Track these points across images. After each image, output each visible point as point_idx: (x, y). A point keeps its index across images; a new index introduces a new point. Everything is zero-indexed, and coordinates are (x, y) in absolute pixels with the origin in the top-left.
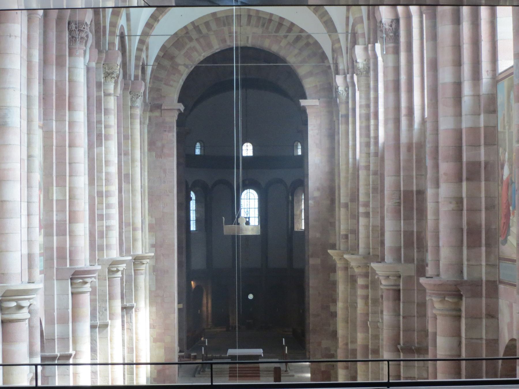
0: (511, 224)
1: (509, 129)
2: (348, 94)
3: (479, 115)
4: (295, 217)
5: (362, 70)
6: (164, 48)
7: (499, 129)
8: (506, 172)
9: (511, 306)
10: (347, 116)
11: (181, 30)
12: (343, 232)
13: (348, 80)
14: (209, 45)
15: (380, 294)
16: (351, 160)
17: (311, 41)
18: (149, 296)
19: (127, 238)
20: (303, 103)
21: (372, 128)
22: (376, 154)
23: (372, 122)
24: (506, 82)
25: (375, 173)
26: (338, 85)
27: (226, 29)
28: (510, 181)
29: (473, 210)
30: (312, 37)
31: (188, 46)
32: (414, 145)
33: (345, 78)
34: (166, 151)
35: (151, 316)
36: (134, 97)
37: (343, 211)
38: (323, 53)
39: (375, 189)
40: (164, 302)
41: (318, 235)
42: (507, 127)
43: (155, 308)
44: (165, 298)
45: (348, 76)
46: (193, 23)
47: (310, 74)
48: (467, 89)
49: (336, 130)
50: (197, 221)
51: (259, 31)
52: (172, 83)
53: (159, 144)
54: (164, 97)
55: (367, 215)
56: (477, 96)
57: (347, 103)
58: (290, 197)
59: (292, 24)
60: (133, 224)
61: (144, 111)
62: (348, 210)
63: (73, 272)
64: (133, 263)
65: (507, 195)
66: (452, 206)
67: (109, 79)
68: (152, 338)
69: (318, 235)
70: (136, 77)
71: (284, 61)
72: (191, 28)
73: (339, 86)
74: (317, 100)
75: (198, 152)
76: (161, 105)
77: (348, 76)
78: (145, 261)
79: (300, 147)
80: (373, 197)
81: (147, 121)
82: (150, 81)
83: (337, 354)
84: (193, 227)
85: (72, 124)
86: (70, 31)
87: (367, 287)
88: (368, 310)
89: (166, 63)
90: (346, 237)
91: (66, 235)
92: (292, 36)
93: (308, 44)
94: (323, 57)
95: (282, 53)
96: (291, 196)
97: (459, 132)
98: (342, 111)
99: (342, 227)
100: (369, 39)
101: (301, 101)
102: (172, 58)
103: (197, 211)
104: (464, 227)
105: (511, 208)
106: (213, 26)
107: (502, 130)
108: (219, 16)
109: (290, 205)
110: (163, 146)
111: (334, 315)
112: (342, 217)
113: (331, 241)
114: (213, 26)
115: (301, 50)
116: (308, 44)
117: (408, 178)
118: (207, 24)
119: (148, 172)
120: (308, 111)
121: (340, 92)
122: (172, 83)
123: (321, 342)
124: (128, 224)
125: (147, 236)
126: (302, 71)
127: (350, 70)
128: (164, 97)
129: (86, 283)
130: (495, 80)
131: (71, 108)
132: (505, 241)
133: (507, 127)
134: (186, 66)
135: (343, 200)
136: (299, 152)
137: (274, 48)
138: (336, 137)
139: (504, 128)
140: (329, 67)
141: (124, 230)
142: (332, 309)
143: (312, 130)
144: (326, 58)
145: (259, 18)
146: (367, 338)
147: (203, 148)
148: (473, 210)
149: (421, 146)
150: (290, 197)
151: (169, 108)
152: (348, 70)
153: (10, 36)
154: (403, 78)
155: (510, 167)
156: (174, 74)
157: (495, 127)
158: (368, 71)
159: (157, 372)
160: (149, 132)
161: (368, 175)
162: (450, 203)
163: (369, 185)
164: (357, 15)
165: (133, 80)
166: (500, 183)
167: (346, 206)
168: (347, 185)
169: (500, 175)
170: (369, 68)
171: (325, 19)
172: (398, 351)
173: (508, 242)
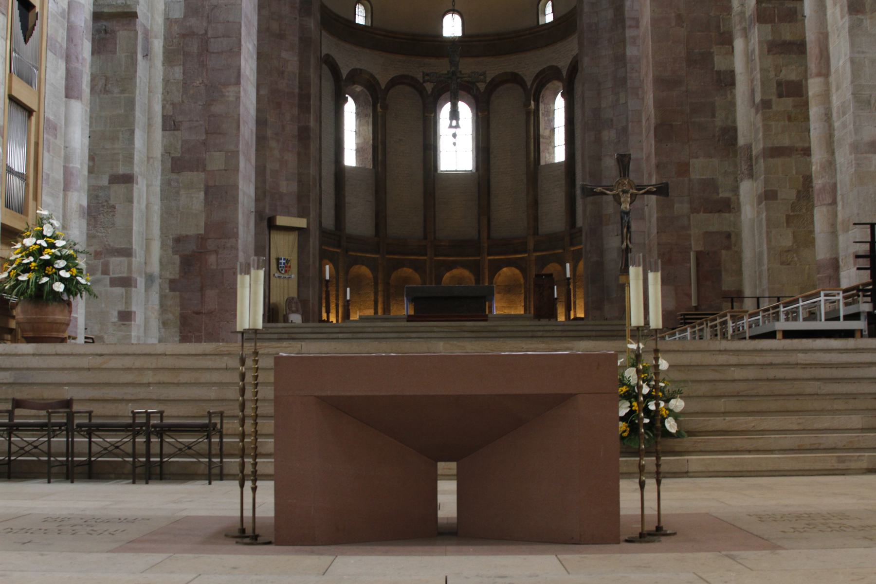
4: (541, 140)
18: (164, 35)
35: (168, 93)
40: (207, 51)
43: (182, 71)
44: (212, 40)
50: (359, 151)
58: (532, 103)
68: (170, 160)
75: (360, 19)
79: (549, 9)
83: (738, 199)
84: (350, 159)
96: (534, 101)
103: (358, 133)
109: (532, 118)
111: (727, 80)
123: (687, 164)
136: (549, 18)
142: (720, 63)
147: (371, 13)
150: (532, 103)
159: (181, 262)
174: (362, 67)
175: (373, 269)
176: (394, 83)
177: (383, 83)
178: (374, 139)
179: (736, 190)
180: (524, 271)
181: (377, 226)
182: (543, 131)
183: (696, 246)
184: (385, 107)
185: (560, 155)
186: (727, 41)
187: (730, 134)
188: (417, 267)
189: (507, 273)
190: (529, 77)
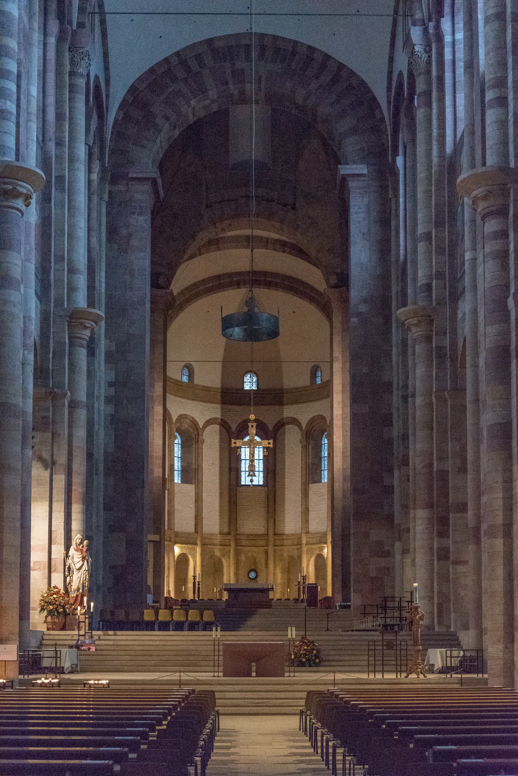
2: (430, 57)
6: (133, 90)
10: (428, 94)
11: (159, 64)
12: (421, 281)
16: (435, 160)
19: (59, 281)
20: (345, 170)
26: (415, 42)
27: (227, 64)
30: (358, 77)
31: (170, 89)
34: (134, 242)
36: (76, 55)
38: (374, 99)
46: (177, 54)
47: (354, 131)
49: (393, 212)
53: (124, 232)
54: (133, 162)
57: (429, 72)
59: (328, 57)
60: (70, 262)
61: (102, 179)
62: (431, 243)
64: (66, 323)
70: (81, 25)
72: (175, 61)
73: (415, 45)
74: (365, 166)
76: (128, 173)
78: (89, 323)
81: (106, 197)
82: (111, 137)
92: (326, 78)
98: (420, 86)
99: (420, 273)
101: (340, 166)
106: (209, 61)
110: (130, 235)
114: (209, 61)
118: (199, 57)
119: (106, 272)
120: (352, 184)
121: (417, 54)
122: (145, 142)
124: (60, 259)
125: (103, 368)
128: (133, 162)
134: (167, 118)
138: (393, 223)
140: (382, 119)
141: (52, 264)
143: (356, 213)
144: (378, 106)
151: (140, 175)
156: (149, 130)
160: (108, 213)
163: (506, 47)
165: (75, 28)
167: (428, 237)
174: (188, 413)
181: (196, 525)
186: (391, 471)
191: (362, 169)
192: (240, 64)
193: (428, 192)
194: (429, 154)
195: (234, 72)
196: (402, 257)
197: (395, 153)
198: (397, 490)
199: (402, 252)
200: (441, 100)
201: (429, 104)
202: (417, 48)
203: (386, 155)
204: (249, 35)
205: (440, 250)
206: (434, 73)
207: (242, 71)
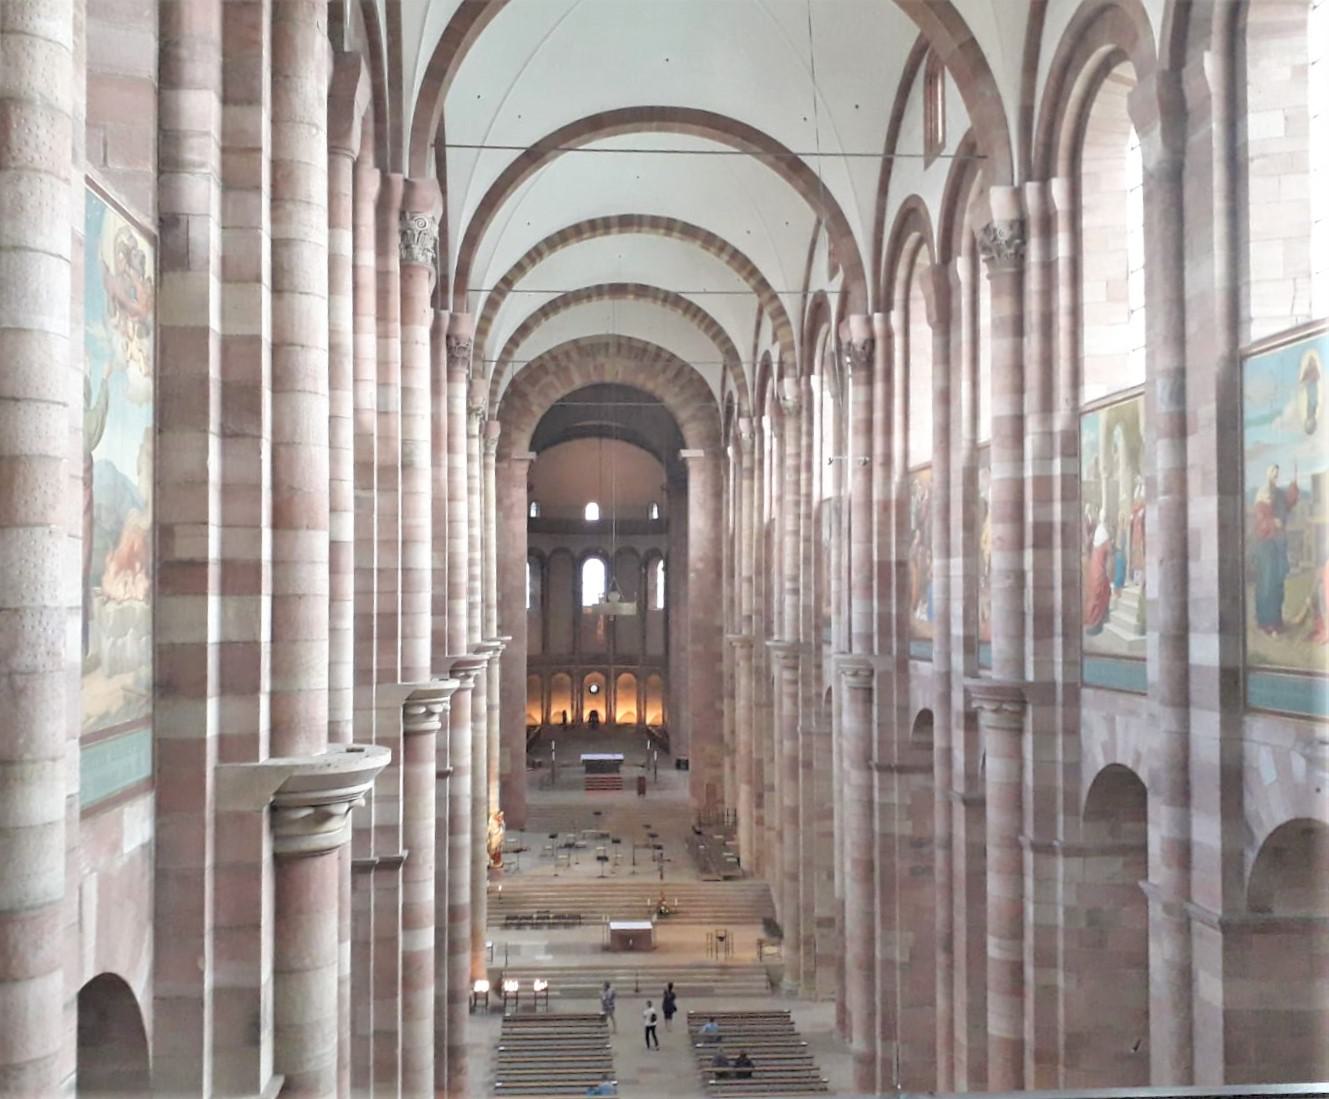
0: (1111, 607)
1: (1110, 475)
3: (1051, 458)
5: (791, 410)
7: (1085, 477)
8: (1100, 536)
9: (1111, 721)
10: (752, 471)
12: (745, 612)
13: (755, 423)
14: (573, 383)
15: (814, 691)
17: (695, 377)
20: (684, 453)
21: (803, 483)
22: (808, 516)
23: (803, 476)
24: (1103, 415)
25: (807, 540)
28: (1109, 548)
29: (1043, 586)
32: (893, 504)
33: (751, 422)
34: (516, 511)
37: (745, 586)
39: (807, 559)
41: (701, 615)
42: (1104, 476)
45: (755, 420)
46: (549, 352)
47: (694, 417)
48: (1032, 425)
49: (725, 487)
51: (632, 364)
52: (523, 426)
55: (796, 591)
56: (1048, 434)
57: (753, 453)
63: (453, 662)
65: (1104, 566)
66: (1009, 582)
67: (474, 414)
69: (701, 615)
71: (660, 400)
72: (547, 357)
77: (755, 420)
79: (655, 509)
80: (804, 569)
85: (451, 471)
86: (449, 349)
87: (795, 682)
88: (797, 711)
89: (517, 403)
90: (750, 618)
91: (444, 613)
92: (670, 373)
93: (691, 380)
94: (710, 396)
95: (658, 393)
97: (1019, 485)
99: (745, 606)
100: (802, 370)
102: (523, 396)
104: (1026, 609)
105: (1112, 586)
107: (1092, 479)
108: (582, 343)
111: (721, 713)
112: (745, 595)
113: (717, 623)
114: (574, 355)
115: (682, 388)
116: (691, 380)
117: (884, 547)
118: (567, 354)
120: (690, 464)
126: (683, 415)
127: (757, 413)
129: (468, 677)
130: (1077, 414)
131: (451, 449)
132: (1098, 629)
133: (1104, 476)
134: (540, 405)
135: (745, 573)
136: (655, 515)
137: (650, 386)
139: (1097, 476)
140: (717, 410)
142: (718, 705)
145: (631, 348)
146: (796, 749)
148: (1043, 586)
149: (903, 505)
152: (754, 411)
153: (417, 343)
154: (878, 415)
155: (1111, 529)
157: (1078, 476)
158: (799, 413)
161: (798, 543)
162: (1008, 577)
164: (787, 340)
166: (1084, 550)
167: (750, 580)
168: (751, 557)
169: (1086, 539)
170: (801, 407)
171: (727, 346)
172: (869, 768)
173: (1105, 631)
175: (541, 676)
176: (555, 552)
177: (547, 553)
178: (542, 590)
179: (722, 759)
180: (636, 676)
181: (543, 647)
182: (650, 587)
183: (706, 781)
184: (548, 570)
185: (660, 604)
187: (721, 738)
188: (569, 673)
189: (625, 677)
190: (642, 553)
191: (700, 453)
192: (601, 359)
193: (751, 546)
194: (751, 517)
195: (595, 368)
196: (731, 531)
197: (727, 445)
198: (726, 713)
199: (731, 525)
200: (761, 477)
201: (752, 478)
202: (744, 435)
203: (719, 440)
204: (608, 336)
205: (759, 594)
206: (756, 456)
207: (602, 365)
